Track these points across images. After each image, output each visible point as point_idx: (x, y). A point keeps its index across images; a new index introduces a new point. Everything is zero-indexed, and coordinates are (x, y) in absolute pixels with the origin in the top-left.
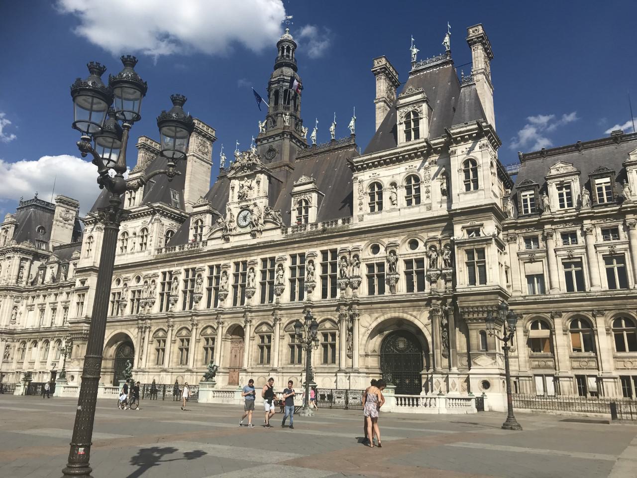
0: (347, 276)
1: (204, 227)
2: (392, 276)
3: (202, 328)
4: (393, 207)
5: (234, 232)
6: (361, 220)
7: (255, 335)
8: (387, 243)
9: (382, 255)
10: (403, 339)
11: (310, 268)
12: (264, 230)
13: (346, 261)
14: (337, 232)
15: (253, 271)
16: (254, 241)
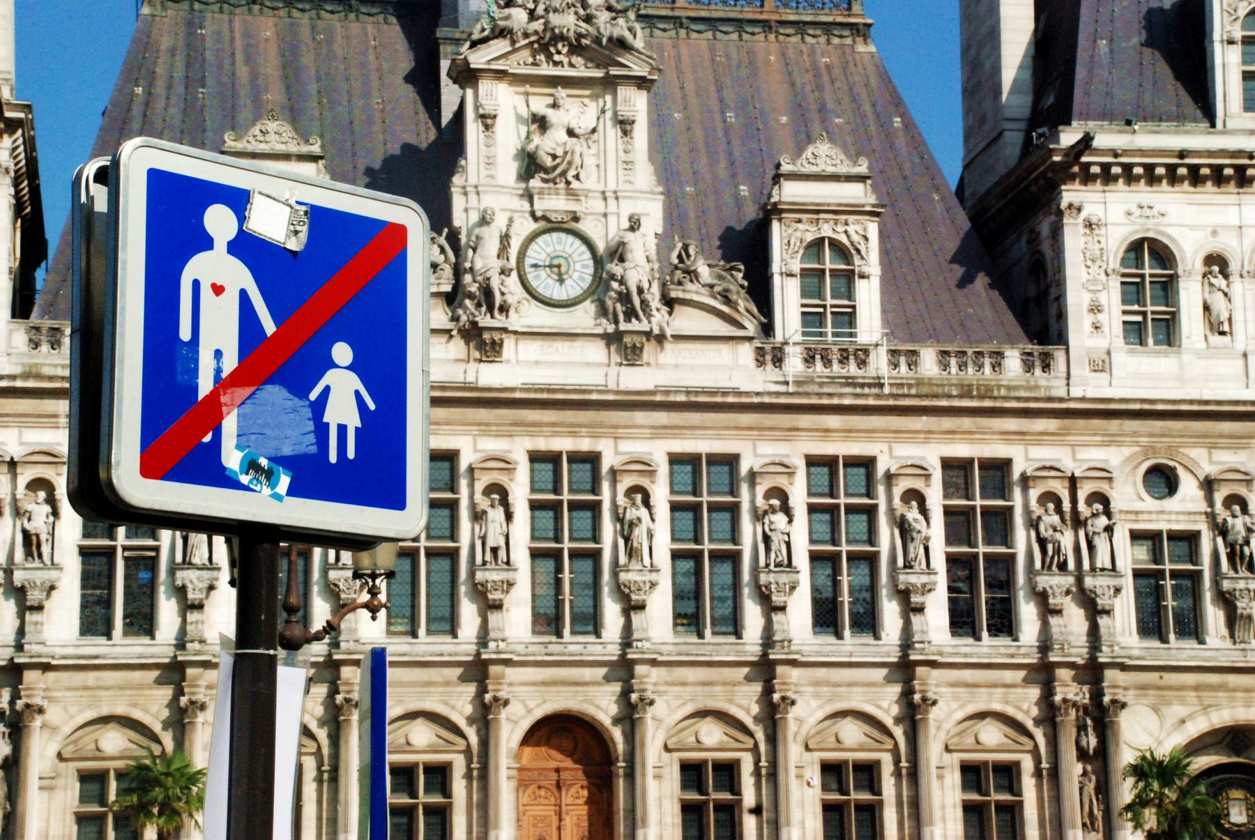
0: (1071, 565)
2: (1241, 585)
4: (1216, 339)
5: (515, 321)
6: (1102, 365)
7: (666, 756)
8: (1208, 468)
9: (1190, 507)
10: (1237, 794)
11: (915, 520)
12: (678, 338)
13: (1059, 510)
14: (1018, 399)
15: (647, 503)
16: (636, 379)
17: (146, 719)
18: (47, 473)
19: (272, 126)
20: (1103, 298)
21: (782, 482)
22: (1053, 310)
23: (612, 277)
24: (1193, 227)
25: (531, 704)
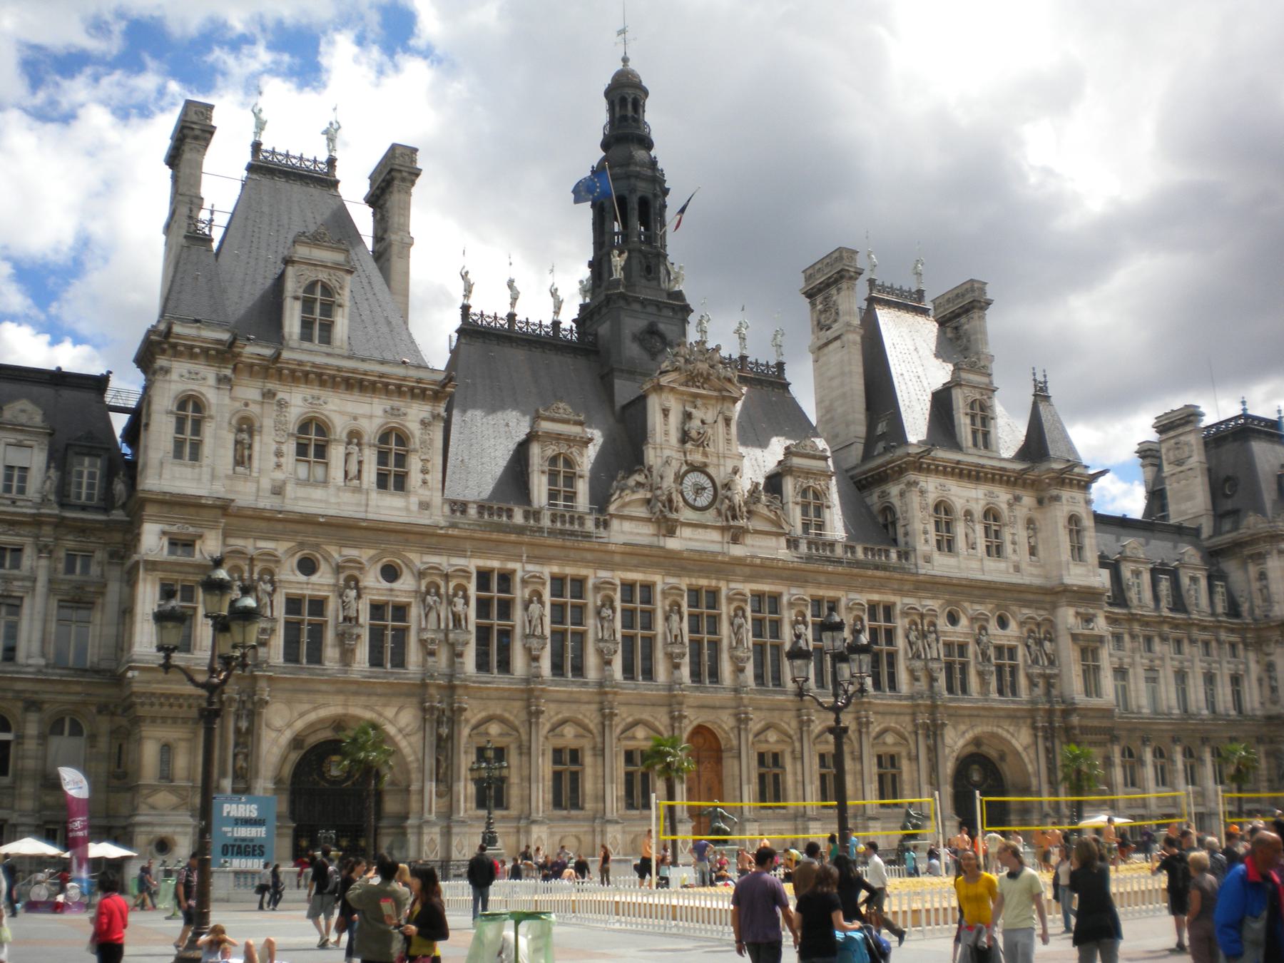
0: (923, 656)
1: (581, 477)
3: (624, 723)
4: (970, 551)
6: (928, 559)
10: (976, 767)
12: (757, 532)
13: (917, 630)
15: (744, 616)
16: (737, 551)
17: (512, 718)
18: (464, 582)
19: (561, 405)
20: (928, 526)
21: (803, 608)
22: (900, 531)
23: (727, 497)
24: (960, 498)
25: (692, 718)
